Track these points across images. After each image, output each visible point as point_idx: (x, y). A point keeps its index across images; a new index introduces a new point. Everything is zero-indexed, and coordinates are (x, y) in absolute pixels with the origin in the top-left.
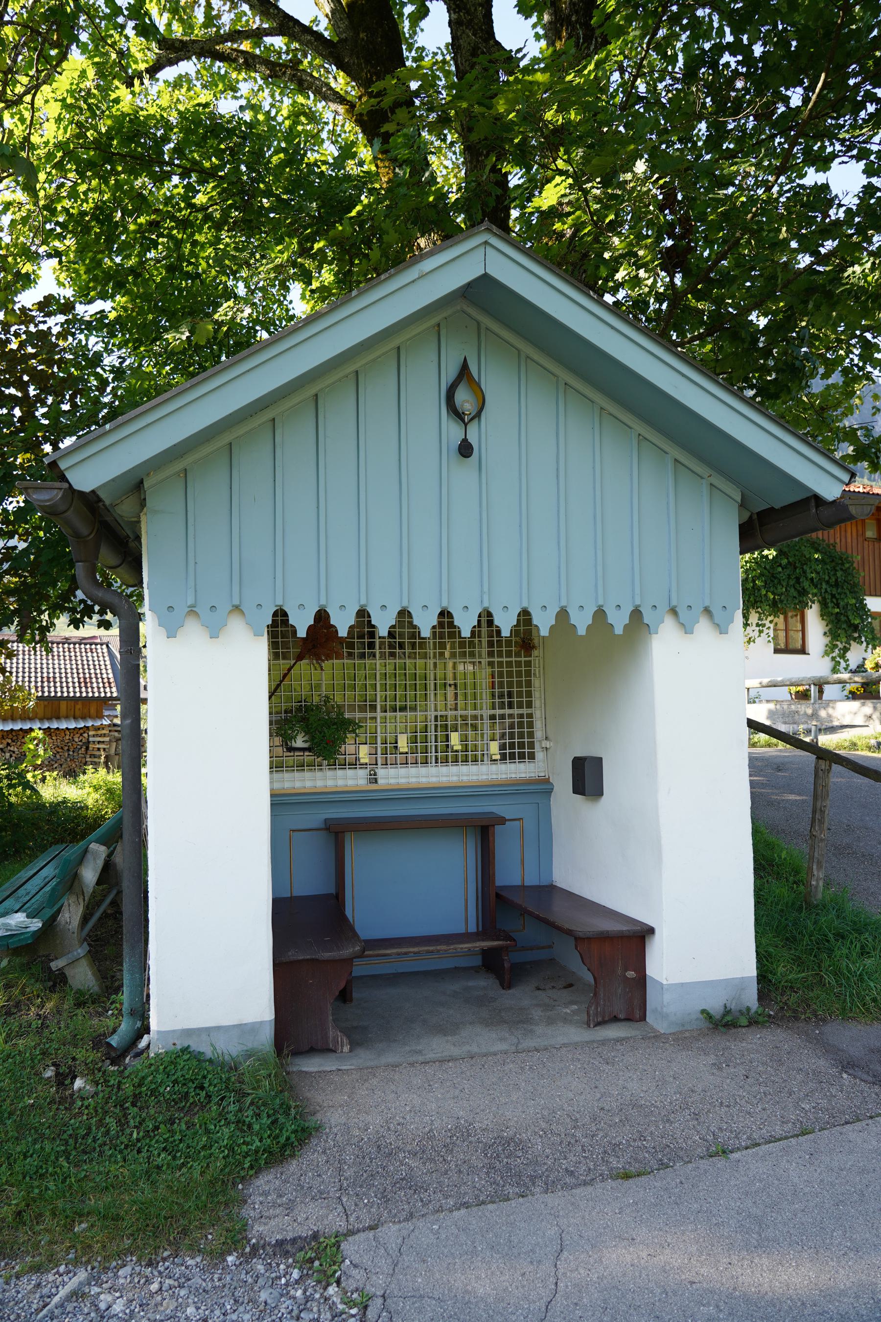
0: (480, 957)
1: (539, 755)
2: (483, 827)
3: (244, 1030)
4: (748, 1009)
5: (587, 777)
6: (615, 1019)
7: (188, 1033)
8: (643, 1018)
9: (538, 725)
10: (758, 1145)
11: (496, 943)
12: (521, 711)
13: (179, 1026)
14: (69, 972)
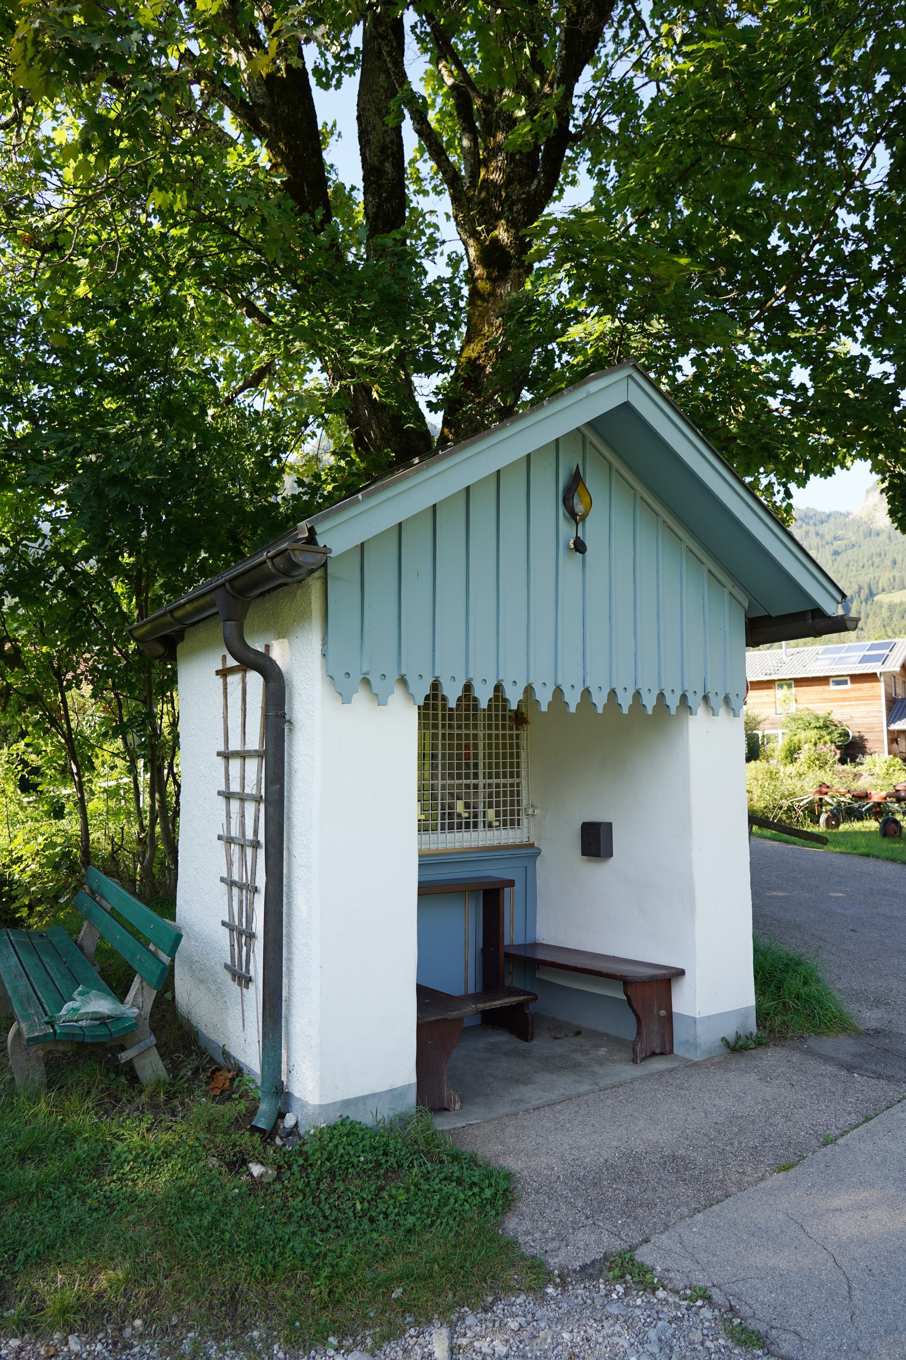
0: (479, 1016)
1: (525, 822)
2: (486, 892)
3: (395, 1094)
4: (751, 1033)
5: (595, 841)
6: (654, 1054)
7: (347, 1103)
8: (671, 1052)
9: (524, 793)
10: (846, 1132)
11: (522, 998)
12: (468, 782)
13: (339, 1098)
14: (138, 1065)
